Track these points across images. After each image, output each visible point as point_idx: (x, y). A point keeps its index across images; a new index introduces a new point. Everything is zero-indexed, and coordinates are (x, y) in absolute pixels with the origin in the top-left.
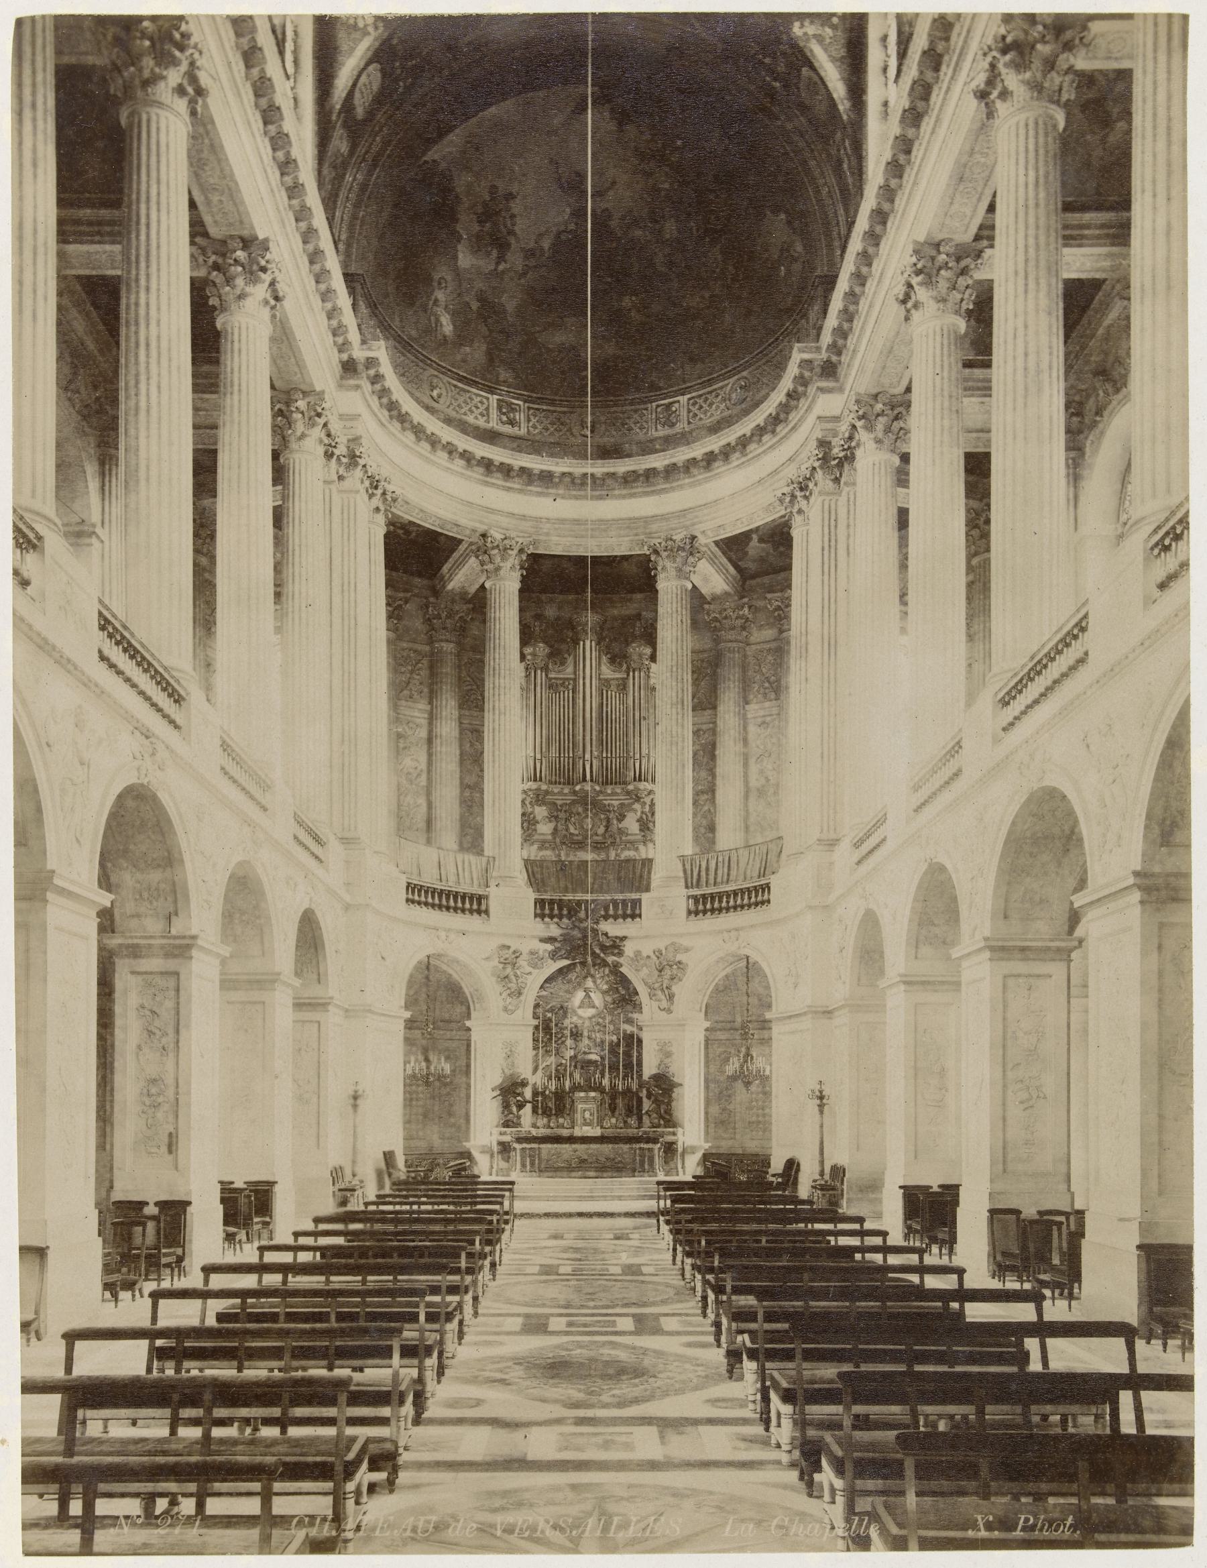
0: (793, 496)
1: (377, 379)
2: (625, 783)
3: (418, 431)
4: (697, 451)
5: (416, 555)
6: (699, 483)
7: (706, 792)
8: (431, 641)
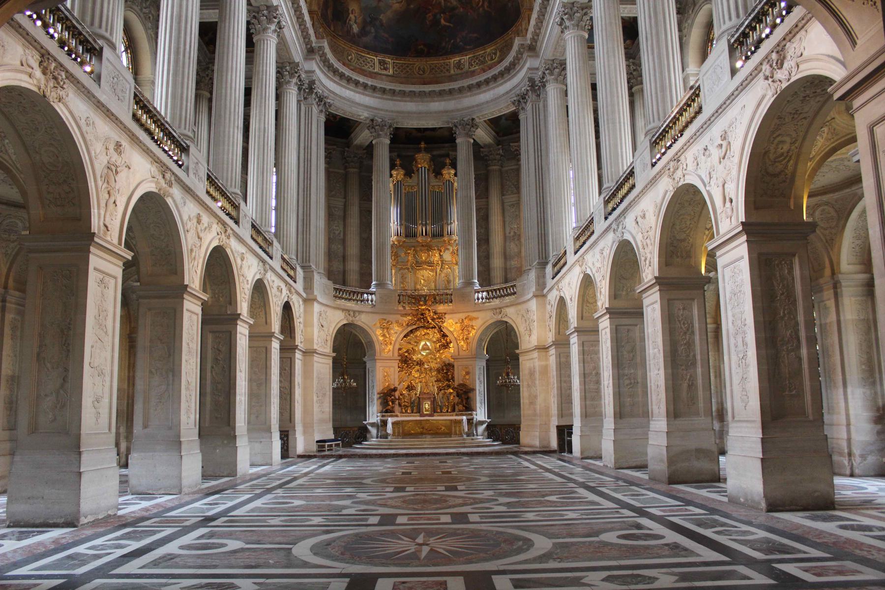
0: (519, 101)
1: (323, 56)
3: (342, 76)
4: (473, 81)
5: (338, 129)
6: (475, 94)
7: (484, 240)
8: (346, 168)
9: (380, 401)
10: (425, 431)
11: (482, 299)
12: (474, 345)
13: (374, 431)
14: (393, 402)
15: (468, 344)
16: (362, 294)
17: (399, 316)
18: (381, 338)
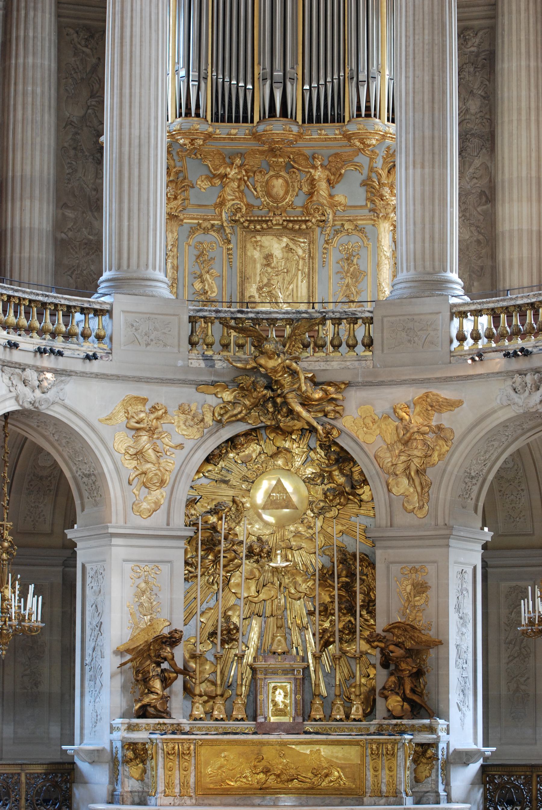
2: (340, 119)
9: (118, 681)
10: (271, 781)
11: (476, 337)
12: (444, 493)
13: (98, 777)
14: (166, 682)
16: (69, 311)
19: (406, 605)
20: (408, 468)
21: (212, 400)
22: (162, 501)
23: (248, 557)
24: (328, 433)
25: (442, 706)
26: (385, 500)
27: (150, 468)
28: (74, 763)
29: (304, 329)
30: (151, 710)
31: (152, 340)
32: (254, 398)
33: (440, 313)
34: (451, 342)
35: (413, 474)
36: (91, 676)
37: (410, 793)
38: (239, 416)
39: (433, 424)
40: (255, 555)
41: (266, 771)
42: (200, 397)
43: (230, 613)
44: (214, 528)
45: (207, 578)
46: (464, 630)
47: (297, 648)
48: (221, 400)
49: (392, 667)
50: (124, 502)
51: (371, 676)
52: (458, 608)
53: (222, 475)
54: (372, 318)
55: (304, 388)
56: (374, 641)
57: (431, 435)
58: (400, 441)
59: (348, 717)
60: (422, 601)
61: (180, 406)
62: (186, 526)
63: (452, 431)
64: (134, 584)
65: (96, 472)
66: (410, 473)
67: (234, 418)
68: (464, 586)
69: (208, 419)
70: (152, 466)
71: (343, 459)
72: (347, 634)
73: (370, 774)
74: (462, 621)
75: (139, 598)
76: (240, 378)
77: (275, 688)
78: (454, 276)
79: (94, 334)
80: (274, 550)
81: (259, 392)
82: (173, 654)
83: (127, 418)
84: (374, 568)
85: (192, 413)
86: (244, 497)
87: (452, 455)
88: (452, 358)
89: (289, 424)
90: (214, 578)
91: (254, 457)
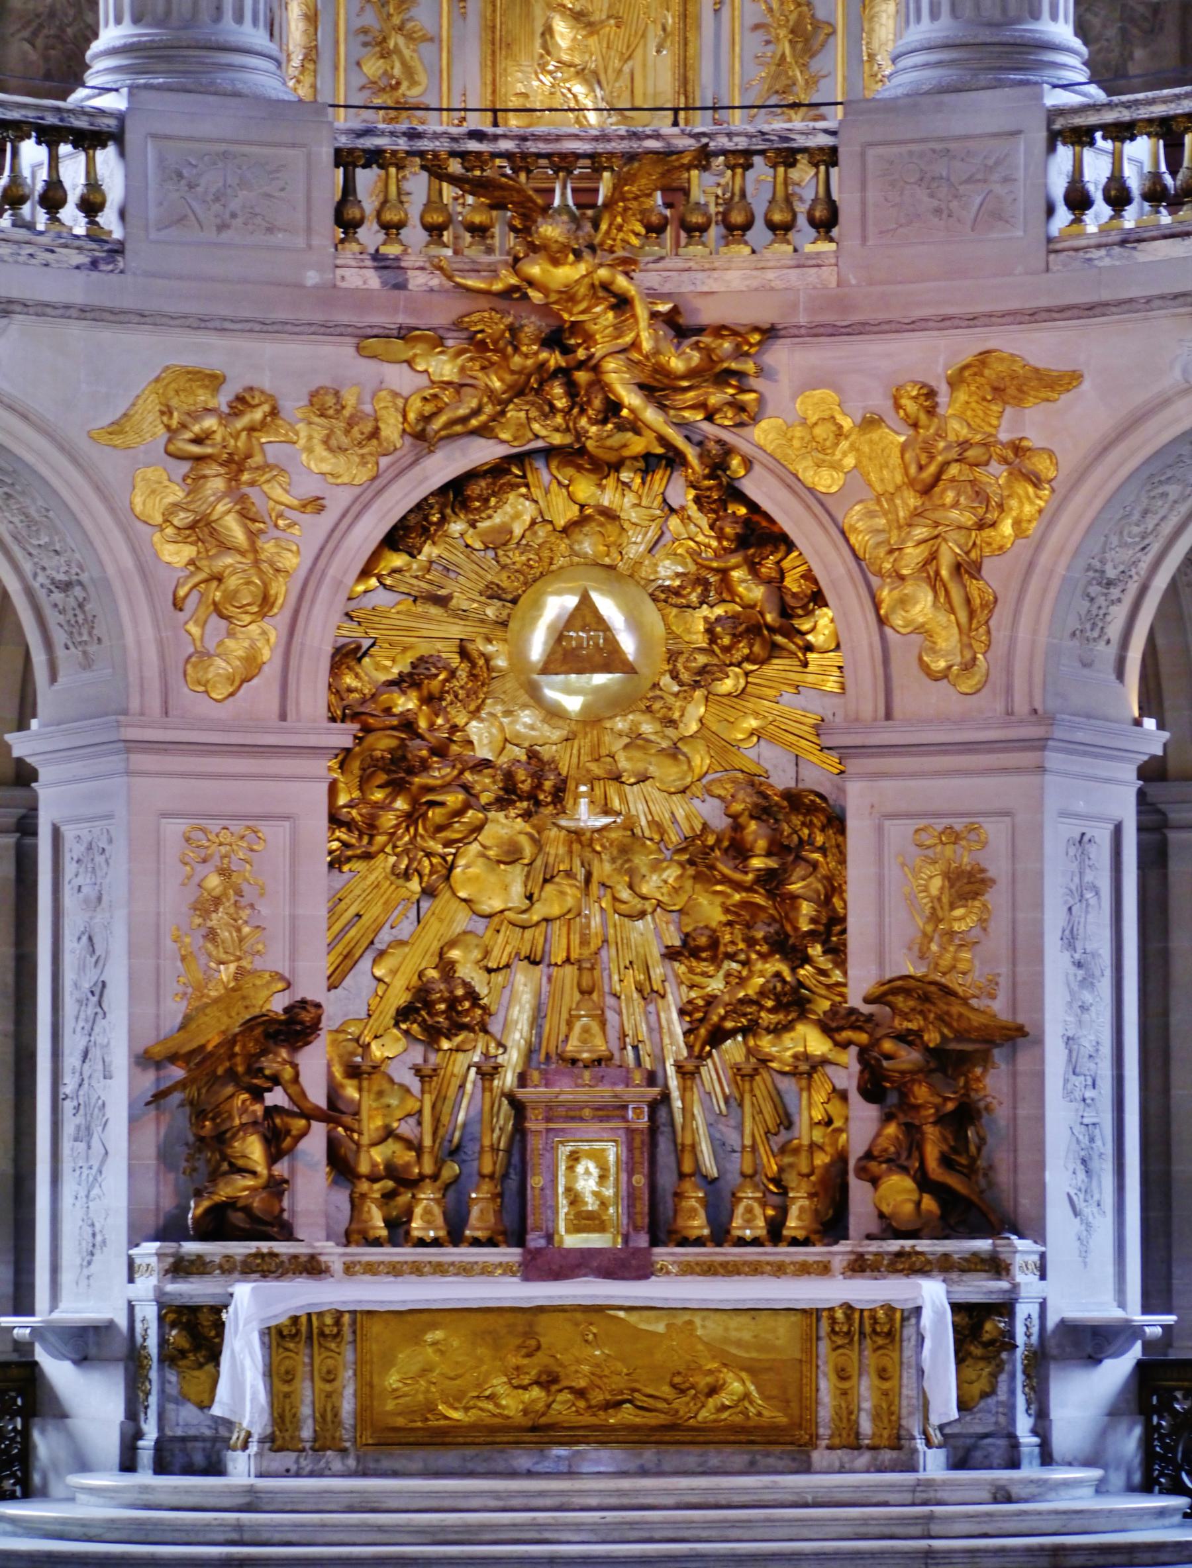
10: (563, 1407)
11: (1118, 197)
13: (92, 1401)
14: (278, 1143)
15: (976, 615)
17: (347, 350)
18: (177, 554)
19: (929, 929)
20: (933, 557)
21: (399, 378)
22: (266, 654)
23: (502, 803)
24: (717, 465)
25: (1025, 1202)
26: (871, 645)
27: (231, 565)
28: (33, 1366)
29: (655, 185)
30: (237, 1218)
31: (234, 215)
32: (513, 372)
33: (1019, 132)
34: (1050, 211)
35: (944, 573)
36: (78, 1127)
37: (937, 1438)
38: (474, 422)
39: (1004, 436)
40: (521, 799)
41: (549, 1381)
42: (367, 369)
43: (455, 954)
44: (408, 725)
45: (393, 859)
46: (1087, 997)
47: (635, 1048)
48: (423, 381)
49: (893, 1098)
50: (162, 657)
51: (838, 1123)
52: (1070, 940)
53: (430, 582)
54: (834, 150)
55: (647, 346)
56: (840, 1029)
57: (995, 467)
58: (911, 483)
59: (775, 1233)
60: (971, 921)
61: (313, 395)
62: (333, 719)
63: (1051, 453)
64: (189, 878)
65: (84, 577)
66: (937, 573)
67: (458, 428)
68: (1089, 877)
69: (391, 430)
70: (239, 558)
71: (759, 537)
72: (771, 1011)
73: (826, 1387)
74: (1081, 973)
75: (206, 914)
76: (475, 317)
77: (574, 1158)
78: (1062, 30)
79: (73, 197)
80: (571, 785)
81: (526, 356)
82: (295, 1066)
83: (168, 427)
84: (842, 831)
85: (346, 413)
86: (489, 640)
87: (1051, 523)
88: (1052, 257)
89: (609, 442)
90: (411, 861)
91: (518, 531)
